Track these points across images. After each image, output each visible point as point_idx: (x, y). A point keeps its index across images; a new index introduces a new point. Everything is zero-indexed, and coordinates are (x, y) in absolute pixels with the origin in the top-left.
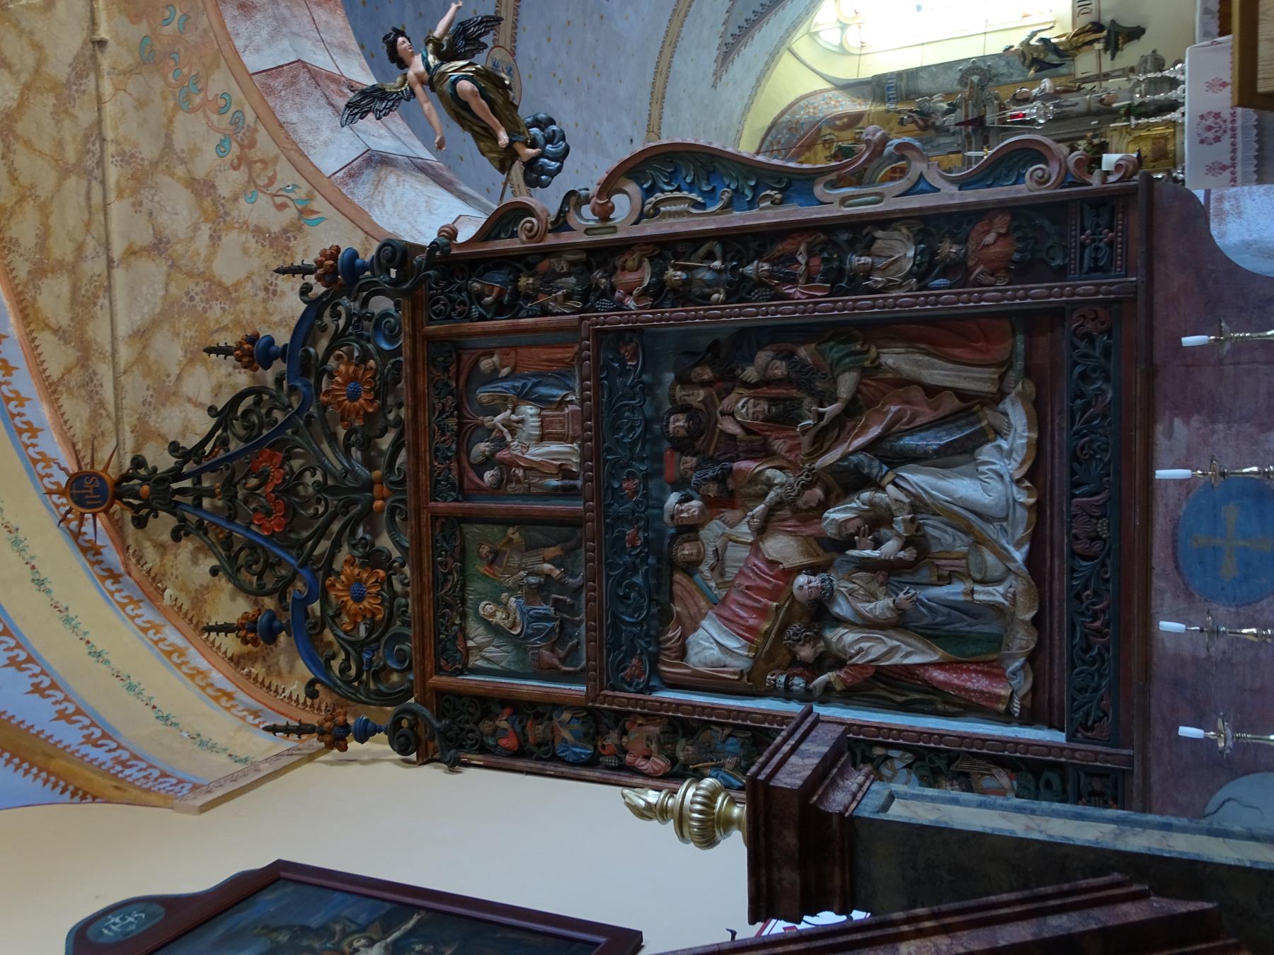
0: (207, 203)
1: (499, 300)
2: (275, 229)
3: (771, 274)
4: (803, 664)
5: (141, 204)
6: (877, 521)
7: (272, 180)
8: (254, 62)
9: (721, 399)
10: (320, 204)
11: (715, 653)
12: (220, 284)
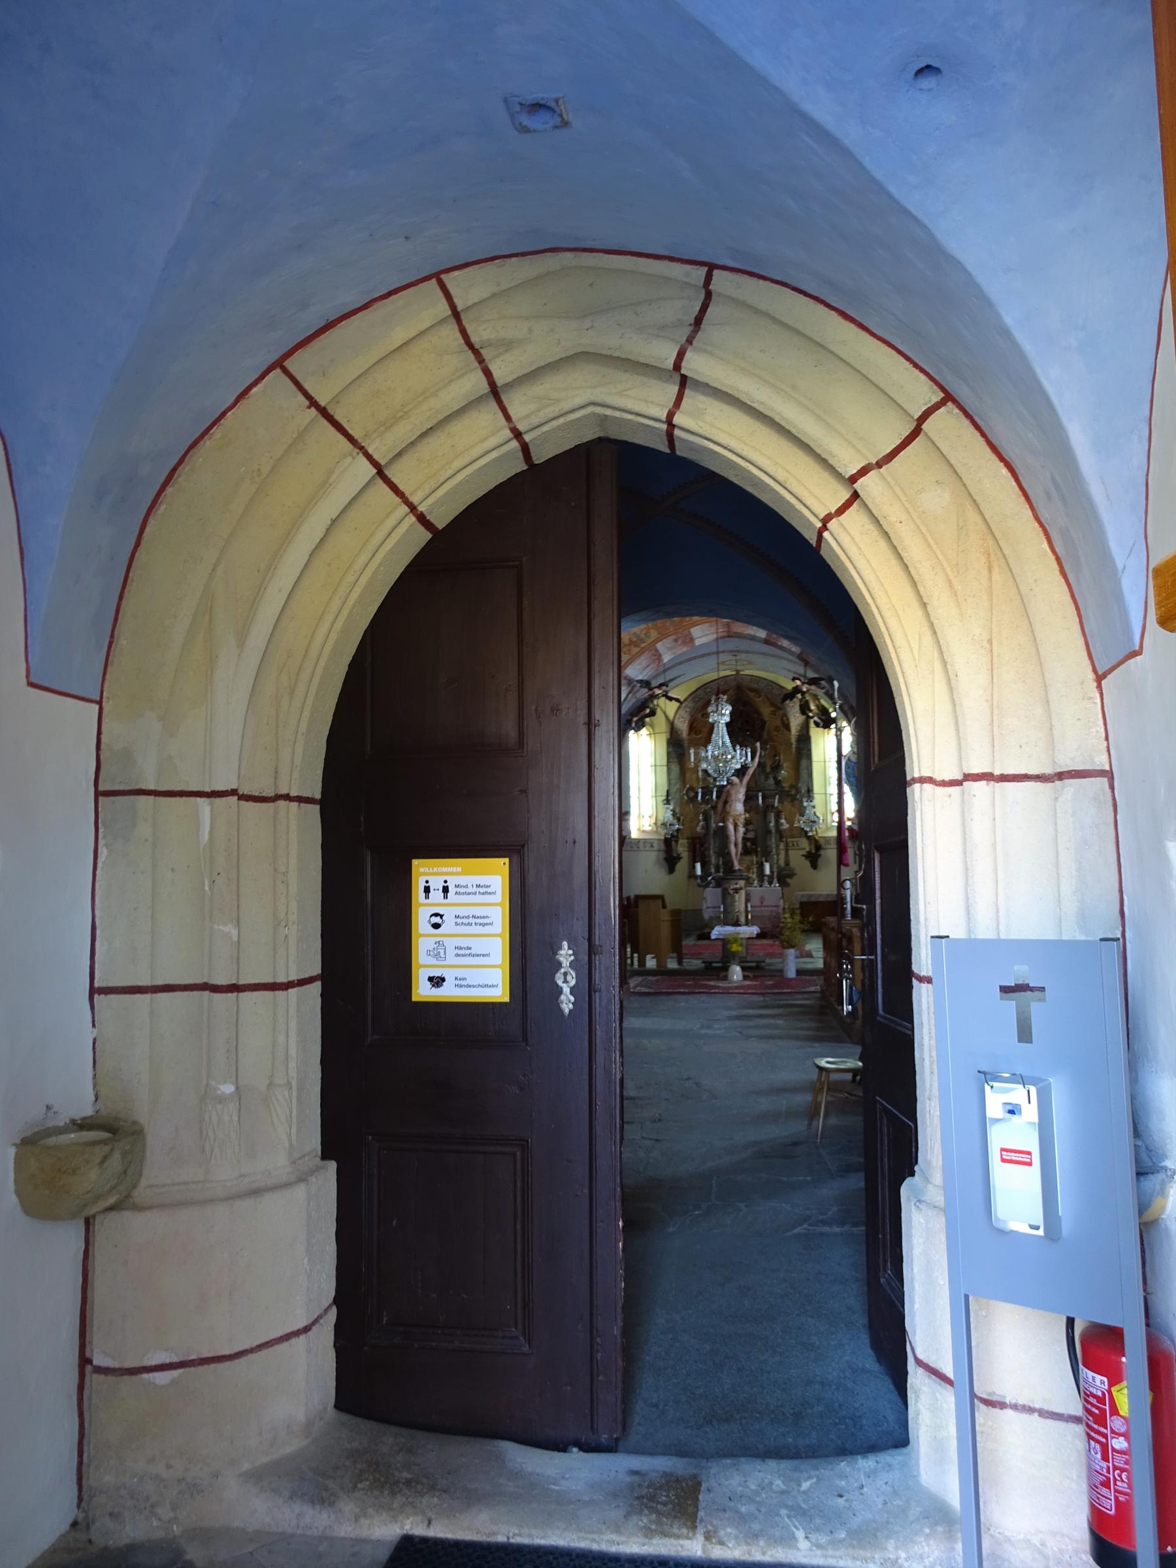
8: (659, 646)
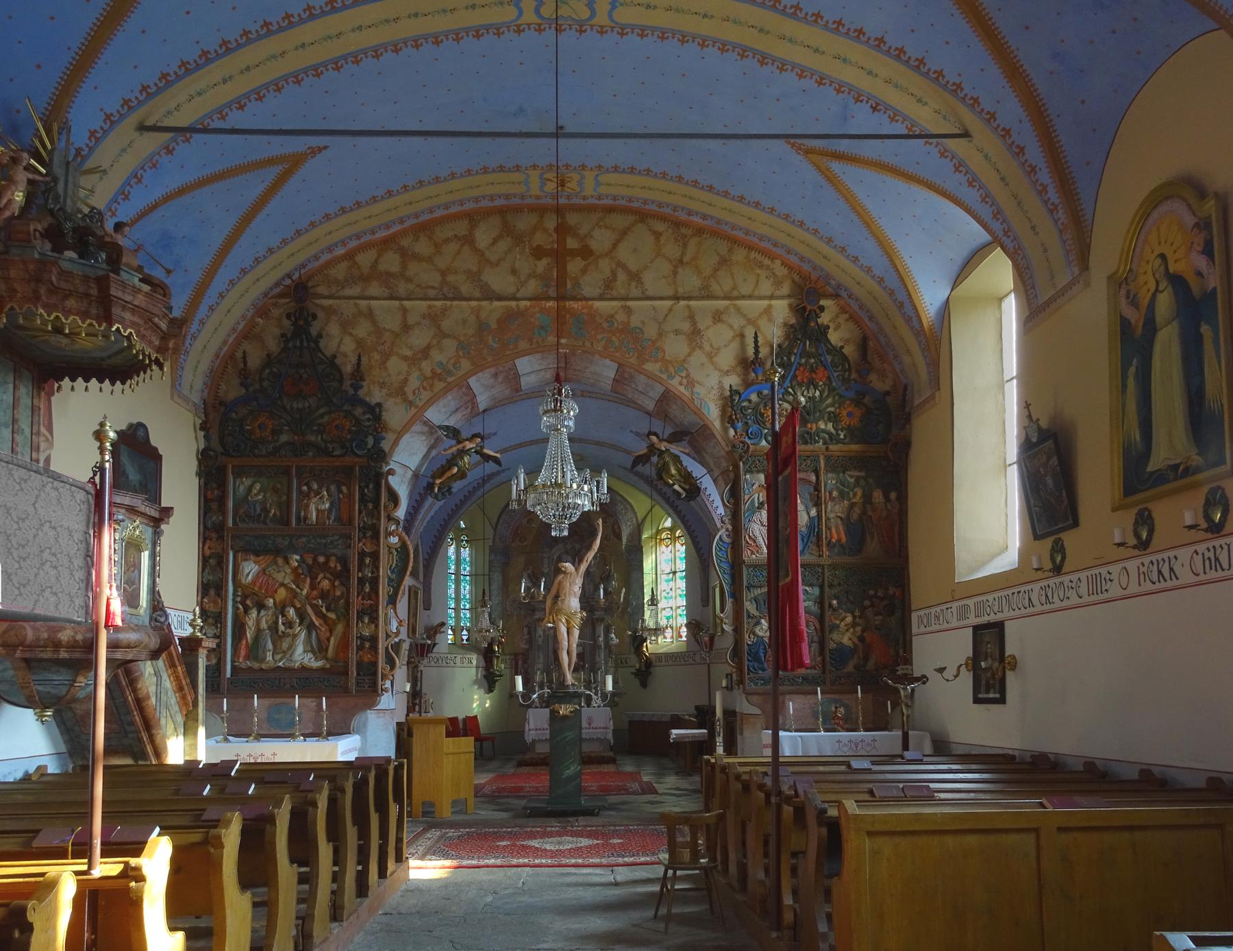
0: (420, 356)
1: (365, 495)
2: (406, 389)
3: (365, 592)
4: (245, 600)
5: (424, 318)
6: (289, 624)
7: (425, 389)
8: (472, 381)
9: (331, 573)
10: (414, 411)
11: (246, 571)
12: (387, 359)
